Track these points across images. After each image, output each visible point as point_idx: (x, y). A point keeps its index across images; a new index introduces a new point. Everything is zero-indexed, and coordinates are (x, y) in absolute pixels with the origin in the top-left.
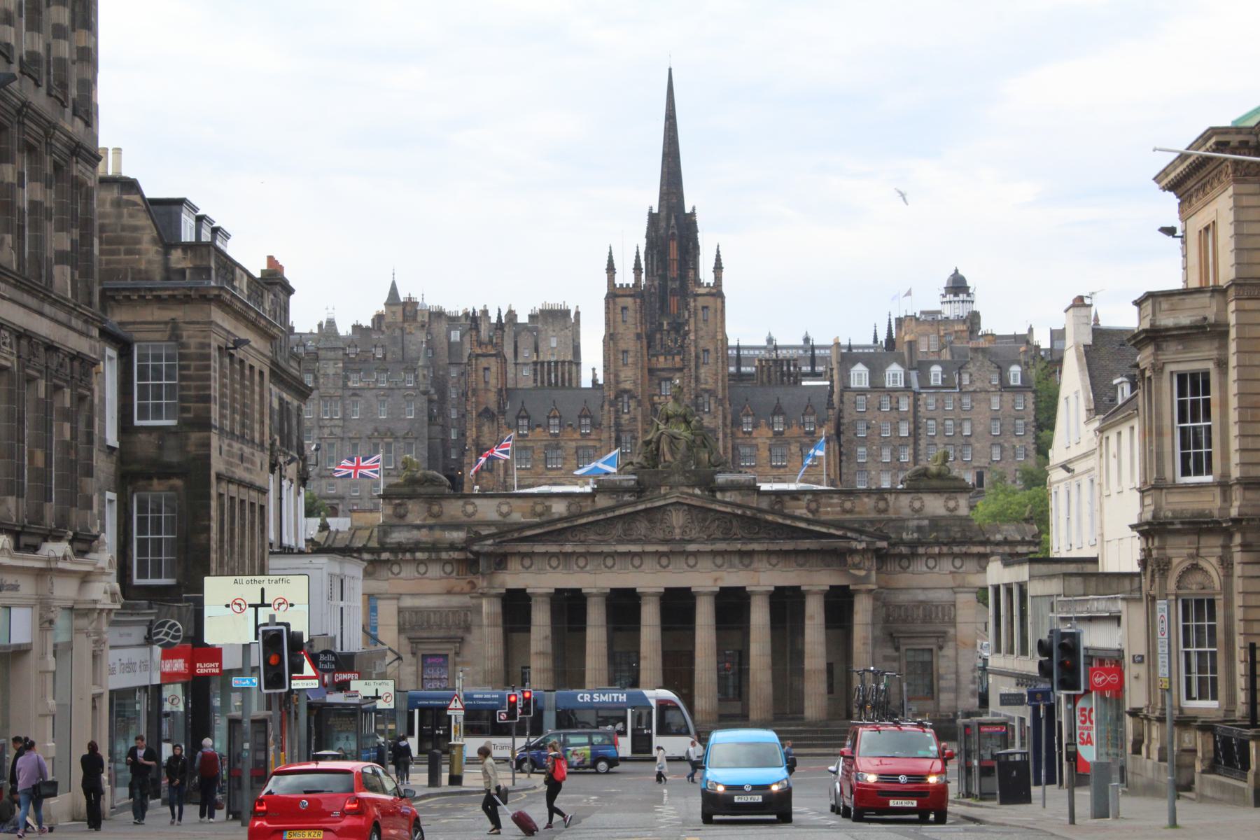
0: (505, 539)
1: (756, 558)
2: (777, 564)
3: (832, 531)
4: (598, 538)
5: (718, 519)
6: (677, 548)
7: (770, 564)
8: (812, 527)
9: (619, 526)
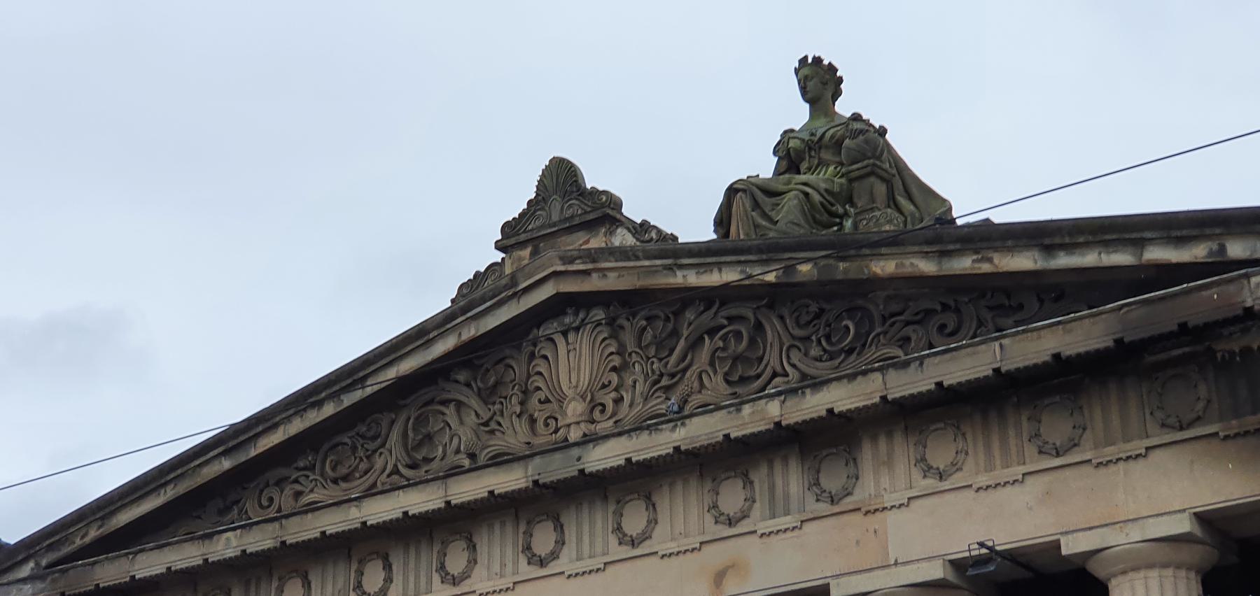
0: (66, 550)
1: (867, 454)
2: (956, 467)
3: (1158, 254)
4: (333, 493)
5: (712, 332)
6: (558, 468)
7: (928, 470)
8: (1064, 261)
9: (395, 436)
